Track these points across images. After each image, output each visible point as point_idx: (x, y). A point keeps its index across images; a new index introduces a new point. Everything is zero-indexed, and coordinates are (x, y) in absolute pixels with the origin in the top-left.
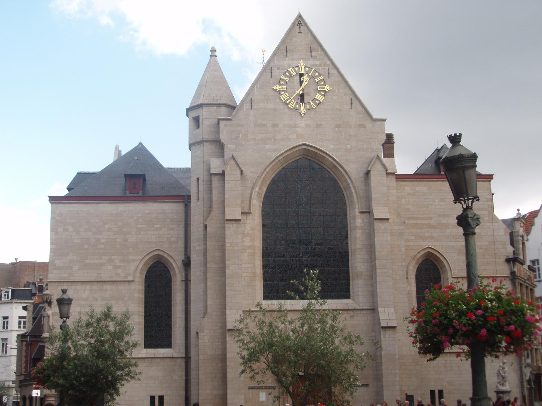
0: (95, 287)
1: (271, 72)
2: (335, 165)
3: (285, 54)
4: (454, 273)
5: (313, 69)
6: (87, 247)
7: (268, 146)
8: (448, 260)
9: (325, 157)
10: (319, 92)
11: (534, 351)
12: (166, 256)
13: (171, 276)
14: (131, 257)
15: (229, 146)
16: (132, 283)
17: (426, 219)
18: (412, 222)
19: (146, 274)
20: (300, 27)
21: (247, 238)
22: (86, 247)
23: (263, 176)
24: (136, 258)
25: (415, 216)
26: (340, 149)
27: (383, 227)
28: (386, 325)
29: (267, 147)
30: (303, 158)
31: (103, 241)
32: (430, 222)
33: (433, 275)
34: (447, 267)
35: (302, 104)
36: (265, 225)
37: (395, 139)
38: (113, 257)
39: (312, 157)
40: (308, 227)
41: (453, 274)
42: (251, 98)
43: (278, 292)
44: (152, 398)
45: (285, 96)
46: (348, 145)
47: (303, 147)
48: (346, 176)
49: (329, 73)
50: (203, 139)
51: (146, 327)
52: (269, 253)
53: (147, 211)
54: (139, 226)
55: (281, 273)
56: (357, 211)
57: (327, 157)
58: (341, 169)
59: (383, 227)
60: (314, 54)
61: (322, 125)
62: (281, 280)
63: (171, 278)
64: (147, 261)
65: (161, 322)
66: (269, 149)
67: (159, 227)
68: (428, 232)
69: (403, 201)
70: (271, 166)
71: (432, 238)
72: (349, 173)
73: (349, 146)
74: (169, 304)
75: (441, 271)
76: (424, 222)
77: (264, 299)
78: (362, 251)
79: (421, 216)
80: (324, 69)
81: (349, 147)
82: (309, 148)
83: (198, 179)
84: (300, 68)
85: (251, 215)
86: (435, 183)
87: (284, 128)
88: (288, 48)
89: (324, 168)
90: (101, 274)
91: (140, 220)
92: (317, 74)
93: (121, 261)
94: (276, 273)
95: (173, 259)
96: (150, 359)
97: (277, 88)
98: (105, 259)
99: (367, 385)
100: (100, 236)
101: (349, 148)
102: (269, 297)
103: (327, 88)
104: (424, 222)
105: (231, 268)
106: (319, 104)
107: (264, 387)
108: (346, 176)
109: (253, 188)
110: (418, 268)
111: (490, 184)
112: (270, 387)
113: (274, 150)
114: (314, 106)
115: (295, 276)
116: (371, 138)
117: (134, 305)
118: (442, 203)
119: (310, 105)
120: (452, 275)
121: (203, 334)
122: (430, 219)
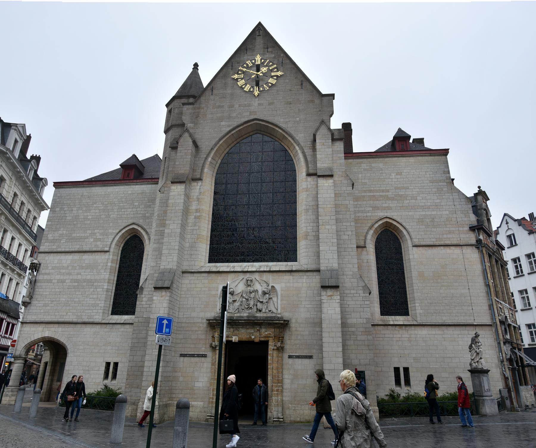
0: (77, 256)
1: (232, 66)
2: (284, 135)
3: (245, 52)
5: (268, 60)
9: (275, 129)
10: (272, 77)
11: (513, 328)
12: (139, 229)
14: (110, 231)
16: (108, 254)
20: (259, 32)
24: (114, 232)
29: (223, 123)
35: (256, 88)
36: (217, 192)
38: (96, 231)
39: (264, 132)
42: (213, 87)
44: (108, 364)
45: (241, 83)
47: (255, 122)
49: (282, 62)
51: (116, 295)
52: (218, 217)
55: (228, 236)
56: (304, 174)
57: (277, 129)
58: (290, 138)
60: (270, 50)
61: (273, 103)
62: (227, 243)
63: (144, 250)
64: (123, 234)
65: (130, 290)
75: (401, 241)
77: (210, 261)
80: (278, 60)
81: (298, 119)
83: (166, 158)
84: (257, 60)
86: (391, 159)
87: (239, 108)
88: (248, 47)
89: (276, 141)
92: (271, 64)
94: (224, 237)
96: (111, 325)
97: (235, 76)
99: (310, 357)
103: (279, 73)
106: (271, 86)
107: (197, 355)
109: (206, 158)
111: (446, 158)
112: (203, 355)
113: (229, 126)
114: (266, 88)
116: (320, 111)
119: (263, 88)
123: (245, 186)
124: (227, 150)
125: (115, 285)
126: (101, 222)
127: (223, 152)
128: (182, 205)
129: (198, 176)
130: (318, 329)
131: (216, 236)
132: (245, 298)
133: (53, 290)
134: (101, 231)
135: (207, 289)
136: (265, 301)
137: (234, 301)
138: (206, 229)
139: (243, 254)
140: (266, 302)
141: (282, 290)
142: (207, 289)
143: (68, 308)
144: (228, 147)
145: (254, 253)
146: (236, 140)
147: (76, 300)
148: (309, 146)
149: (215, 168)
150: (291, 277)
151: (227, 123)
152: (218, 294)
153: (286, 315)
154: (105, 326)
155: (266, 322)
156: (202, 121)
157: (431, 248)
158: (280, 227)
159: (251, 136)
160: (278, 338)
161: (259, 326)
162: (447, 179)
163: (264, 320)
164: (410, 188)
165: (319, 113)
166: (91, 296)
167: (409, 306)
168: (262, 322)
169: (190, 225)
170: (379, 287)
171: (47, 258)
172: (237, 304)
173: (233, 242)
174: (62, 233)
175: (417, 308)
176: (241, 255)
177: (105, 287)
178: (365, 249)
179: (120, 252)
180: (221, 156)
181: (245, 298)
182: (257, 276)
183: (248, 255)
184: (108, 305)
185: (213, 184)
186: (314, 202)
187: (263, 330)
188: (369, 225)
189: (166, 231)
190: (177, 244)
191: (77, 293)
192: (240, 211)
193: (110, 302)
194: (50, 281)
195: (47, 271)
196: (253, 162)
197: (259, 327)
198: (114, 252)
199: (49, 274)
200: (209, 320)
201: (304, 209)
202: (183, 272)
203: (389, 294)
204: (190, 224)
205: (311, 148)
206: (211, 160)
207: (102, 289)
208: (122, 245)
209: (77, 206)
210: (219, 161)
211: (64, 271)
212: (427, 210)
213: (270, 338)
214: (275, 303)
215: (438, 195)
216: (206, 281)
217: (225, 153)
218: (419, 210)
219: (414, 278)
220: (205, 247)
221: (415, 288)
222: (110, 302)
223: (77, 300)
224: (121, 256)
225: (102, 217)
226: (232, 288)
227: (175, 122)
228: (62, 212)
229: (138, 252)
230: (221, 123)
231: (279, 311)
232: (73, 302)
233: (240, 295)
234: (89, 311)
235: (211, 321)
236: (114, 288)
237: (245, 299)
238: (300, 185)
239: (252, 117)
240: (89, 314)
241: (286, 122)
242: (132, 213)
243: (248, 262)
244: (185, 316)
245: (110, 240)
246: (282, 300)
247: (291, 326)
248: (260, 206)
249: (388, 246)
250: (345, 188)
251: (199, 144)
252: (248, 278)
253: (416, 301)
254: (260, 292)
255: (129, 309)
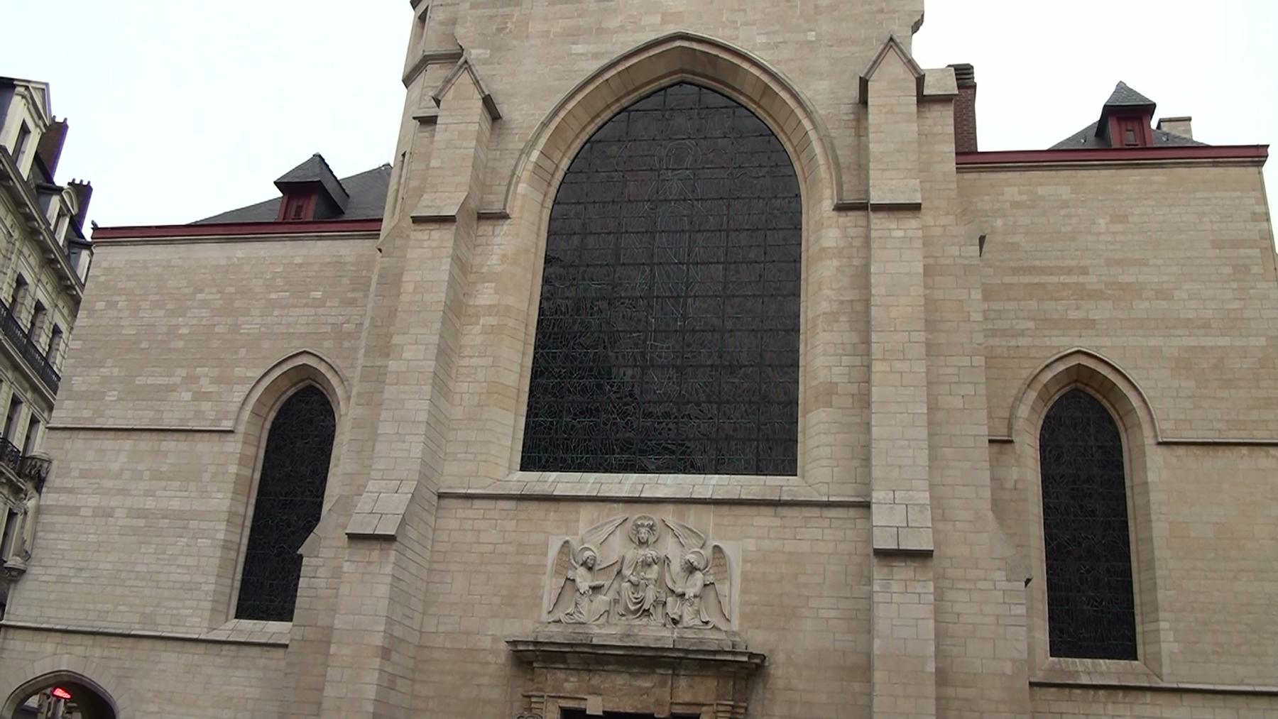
0: (145, 443)
2: (767, 86)
4: (1161, 430)
6: (147, 347)
7: (580, 46)
8: (1141, 390)
12: (322, 368)
13: (334, 426)
14: (239, 371)
15: (474, 52)
16: (230, 437)
17: (1069, 271)
18: (1026, 279)
19: (276, 418)
21: (486, 285)
22: (144, 345)
23: (557, 120)
24: (249, 374)
25: (1037, 263)
26: (785, 42)
27: (900, 233)
28: (892, 545)
29: (578, 49)
30: (680, 83)
31: (183, 331)
32: (1082, 279)
33: (1097, 440)
34: (1141, 413)
37: (978, 78)
40: (681, 263)
41: (1159, 433)
43: (567, 450)
46: (810, 30)
47: (678, 43)
48: (800, 113)
50: (425, 54)
52: (555, 334)
53: (298, 260)
54: (273, 296)
55: (584, 390)
56: (828, 204)
57: (745, 65)
58: (783, 94)
59: (900, 233)
62: (581, 413)
63: (334, 431)
66: (582, 54)
67: (319, 297)
68: (1078, 308)
69: (999, 223)
70: (579, 97)
71: (1089, 324)
72: (808, 103)
73: (814, 33)
74: (319, 500)
76: (1063, 279)
77: (523, 468)
78: (837, 321)
79: (1054, 263)
81: (811, 36)
82: (695, 46)
83: (404, 155)
85: (508, 222)
90: (162, 411)
91: (278, 280)
93: (214, 381)
94: (570, 392)
95: (339, 375)
98: (182, 372)
100: (180, 319)
101: (814, 39)
102: (539, 461)
104: (1063, 279)
105: (404, 355)
108: (800, 113)
109: (525, 152)
110: (1047, 417)
111: (1260, 173)
113: (596, 56)
115: (625, 400)
117: (220, 495)
118: (1119, 227)
120: (1156, 436)
121: (314, 561)
122: (1084, 271)
123: (641, 240)
124: (592, 129)
125: (247, 532)
126: (215, 344)
127: (577, 136)
128: (444, 286)
129: (497, 208)
130: (856, 687)
131: (546, 390)
132: (629, 581)
133: (83, 537)
134: (216, 372)
135: (512, 549)
136: (690, 593)
137: (596, 589)
138: (517, 368)
139: (626, 446)
140: (695, 596)
141: (745, 561)
142: (512, 549)
143: (119, 591)
144: (593, 120)
145: (660, 444)
146: (618, 100)
147: (138, 568)
148: (846, 118)
149: (549, 184)
150: (777, 522)
151: (592, 48)
152: (545, 566)
153: (757, 640)
154: (216, 648)
155: (690, 656)
156: (515, 42)
157: (1211, 451)
158: (745, 366)
159: (664, 89)
160: (729, 708)
161: (669, 668)
162: (1262, 238)
163: (687, 651)
164: (1152, 262)
165: (880, 16)
166: (181, 560)
167: (1139, 628)
168: (681, 655)
169: (466, 354)
170: (1049, 568)
171: (68, 445)
172: (602, 599)
173: (597, 410)
174: (109, 374)
175: (1163, 635)
176: (622, 449)
177: (221, 536)
178: (1008, 446)
179: (265, 435)
180: (569, 147)
181: (629, 581)
182: (668, 515)
183: (643, 452)
184: (227, 590)
185: (544, 234)
186: (857, 291)
187: (683, 683)
188: (1026, 373)
189: (393, 365)
190: (425, 405)
191: (143, 550)
192: (624, 316)
193: (233, 579)
194: (73, 511)
195: (68, 483)
196: (667, 169)
197: (670, 672)
198: (246, 434)
199: (71, 491)
200: (514, 643)
201: (824, 313)
202: (441, 496)
203: (1079, 591)
204: (469, 349)
205: (850, 124)
206: (538, 158)
207: (210, 541)
208: (273, 415)
209: (151, 298)
210: (565, 165)
211: (108, 483)
212: (1202, 331)
213: (704, 709)
214: (721, 599)
215: (1235, 285)
216: (511, 525)
217: (584, 140)
218: (1179, 332)
219: (1156, 542)
220: (511, 422)
221: (1158, 573)
222: (233, 579)
223: (144, 568)
224: (267, 446)
225: (218, 329)
226: (590, 549)
227: (433, 48)
228: (112, 313)
229: (316, 436)
230: (574, 46)
231: (735, 625)
232: (133, 575)
233: (616, 569)
234: (174, 604)
235: (521, 648)
236: (245, 541)
237: (628, 584)
238: (812, 239)
239: (671, 29)
240: (175, 612)
241: (777, 45)
242: (302, 320)
243: (644, 470)
244: (441, 628)
245: (238, 398)
246: (744, 591)
247: (772, 672)
248: (685, 304)
249: (1080, 443)
250: (955, 251)
251: (503, 109)
252: (640, 518)
253: (1162, 615)
254: (676, 566)
255: (285, 602)
